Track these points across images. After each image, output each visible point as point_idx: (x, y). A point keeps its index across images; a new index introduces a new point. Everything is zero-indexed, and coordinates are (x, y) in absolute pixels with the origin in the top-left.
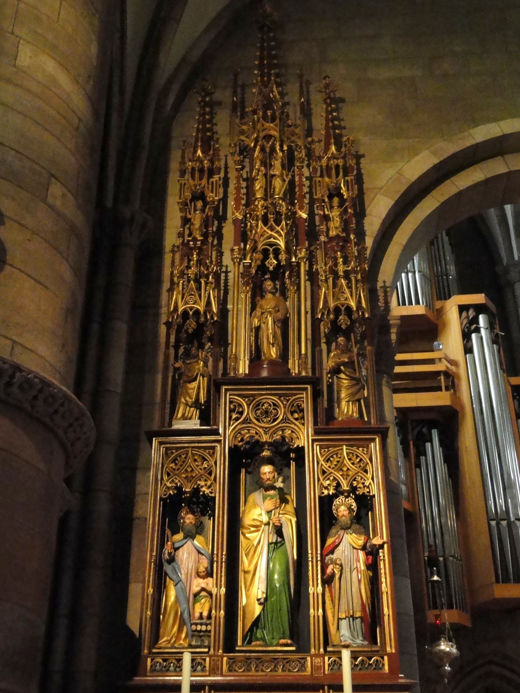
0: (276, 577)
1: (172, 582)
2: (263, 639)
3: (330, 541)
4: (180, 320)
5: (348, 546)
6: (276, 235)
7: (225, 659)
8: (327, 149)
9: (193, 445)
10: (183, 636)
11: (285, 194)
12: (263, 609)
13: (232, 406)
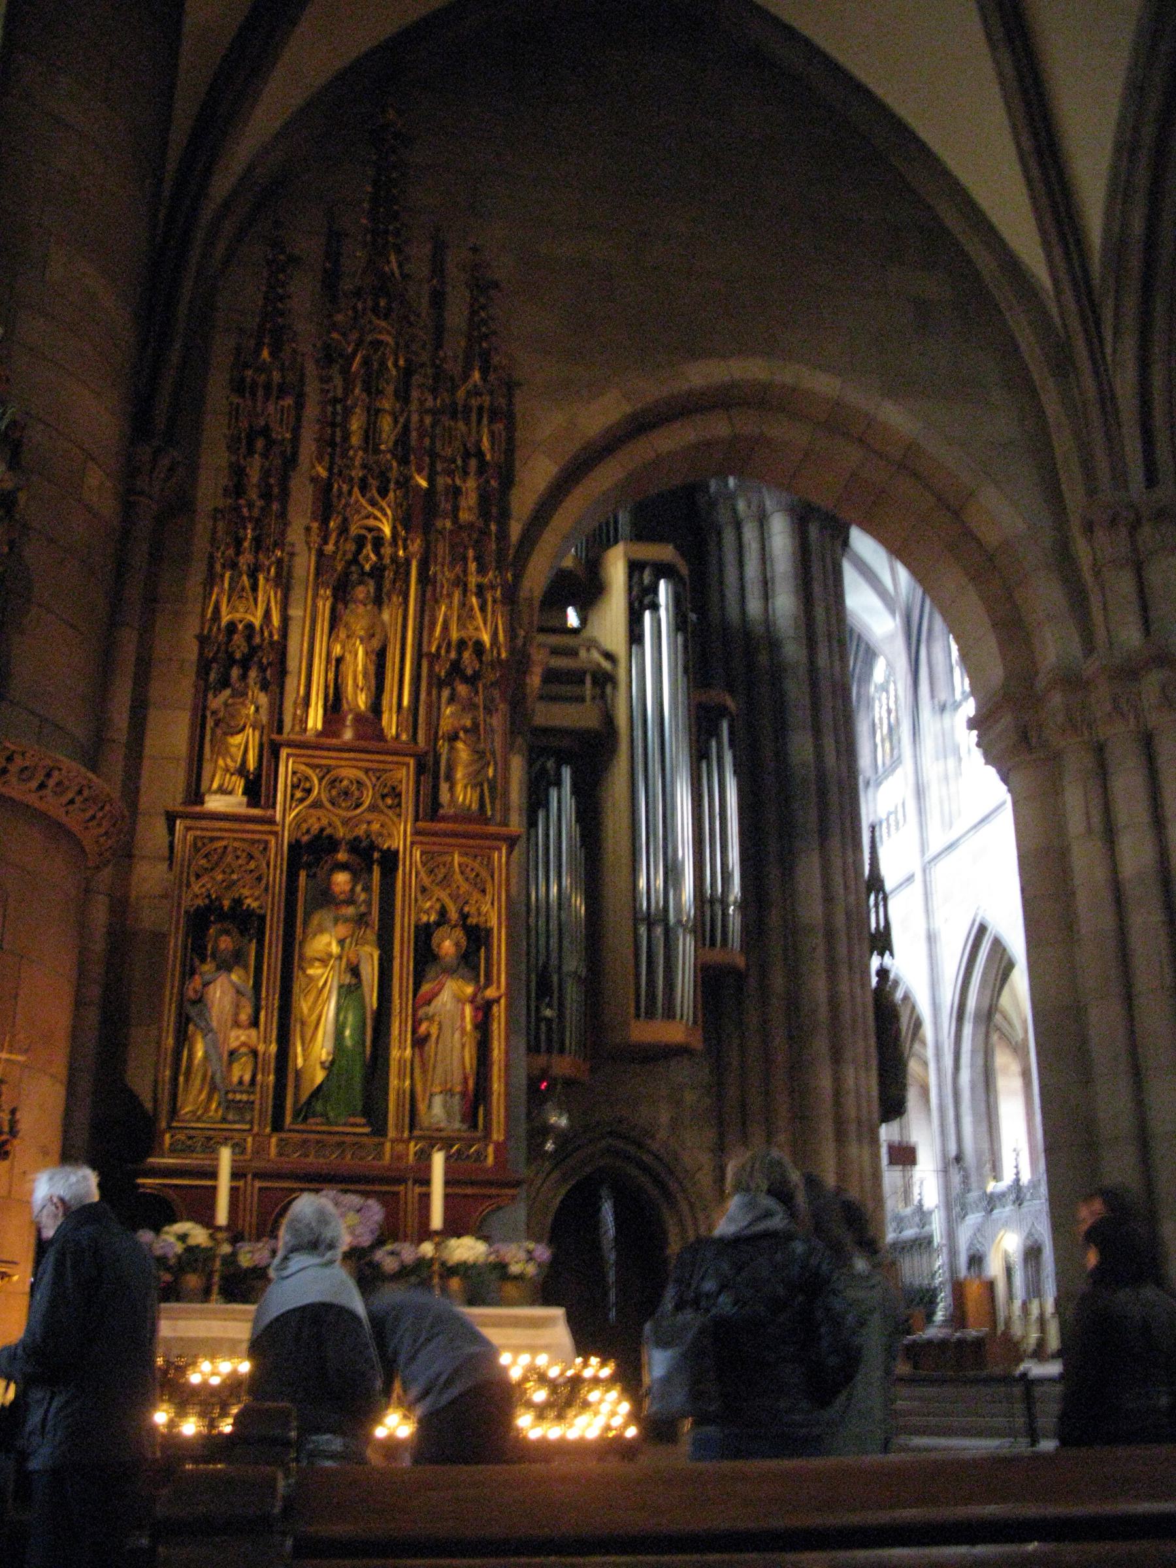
0: (347, 1033)
1: (198, 1032)
2: (324, 1115)
3: (426, 988)
4: (221, 638)
5: (451, 998)
6: (379, 514)
7: (274, 1140)
8: (466, 376)
9: (235, 835)
10: (214, 1106)
11: (396, 443)
12: (328, 1076)
13: (295, 780)
